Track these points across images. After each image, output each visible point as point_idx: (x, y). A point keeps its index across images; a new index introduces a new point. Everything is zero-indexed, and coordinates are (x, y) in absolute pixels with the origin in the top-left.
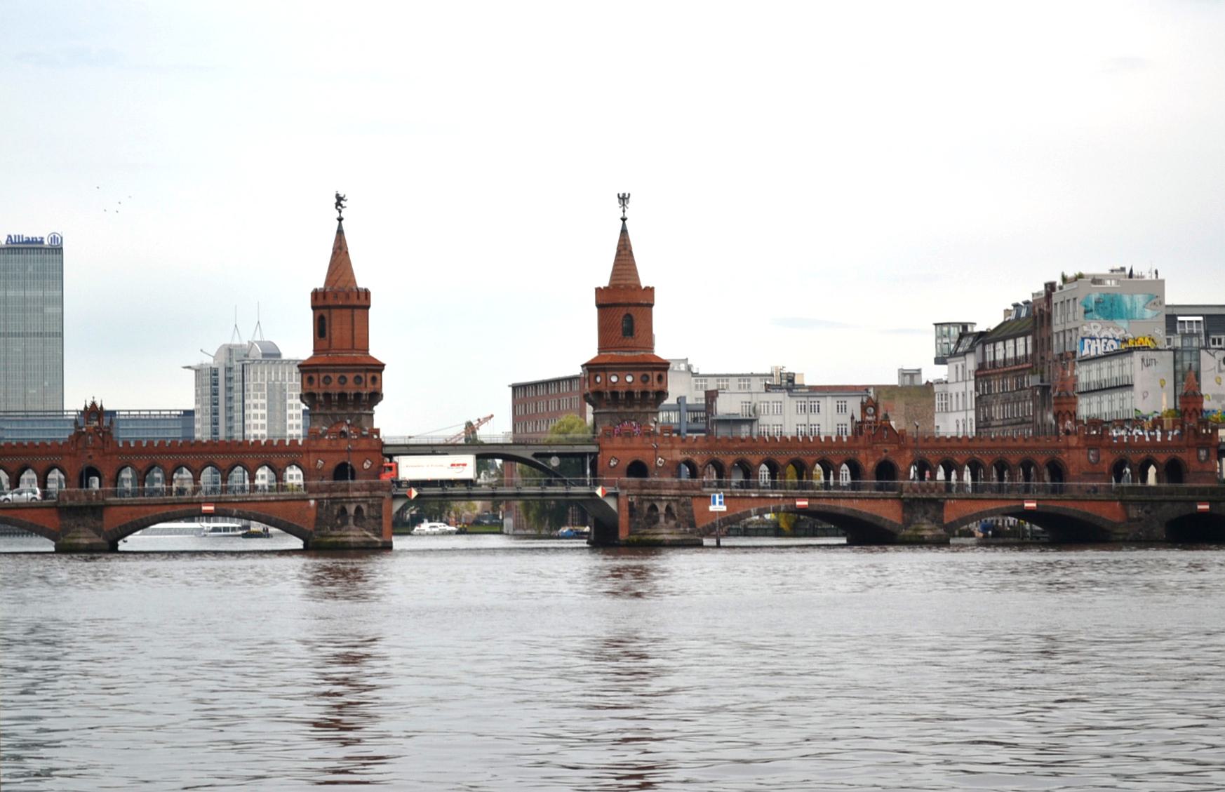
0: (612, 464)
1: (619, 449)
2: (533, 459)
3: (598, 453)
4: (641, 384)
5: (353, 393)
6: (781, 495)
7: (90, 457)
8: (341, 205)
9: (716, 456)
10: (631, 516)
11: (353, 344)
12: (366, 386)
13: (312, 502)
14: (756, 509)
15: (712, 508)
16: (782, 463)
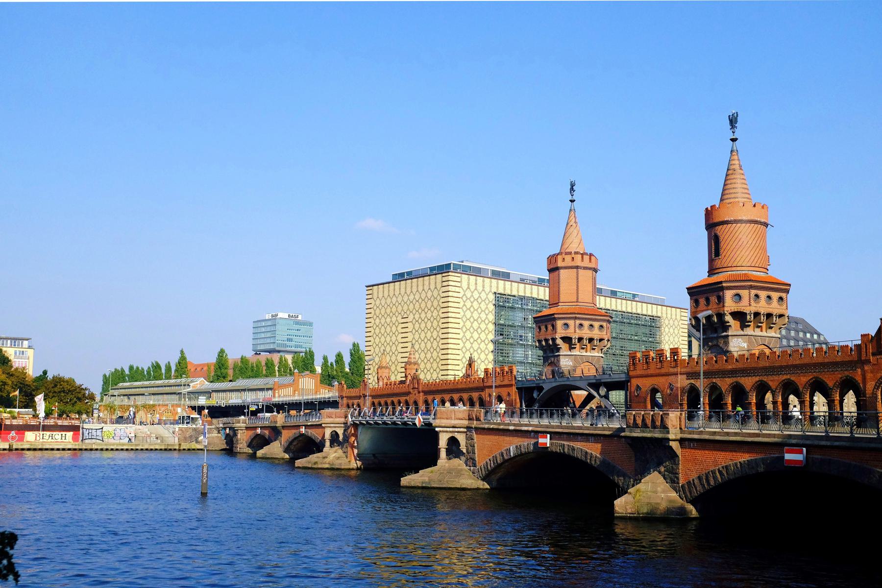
5: (550, 338)
8: (573, 189)
14: (514, 446)
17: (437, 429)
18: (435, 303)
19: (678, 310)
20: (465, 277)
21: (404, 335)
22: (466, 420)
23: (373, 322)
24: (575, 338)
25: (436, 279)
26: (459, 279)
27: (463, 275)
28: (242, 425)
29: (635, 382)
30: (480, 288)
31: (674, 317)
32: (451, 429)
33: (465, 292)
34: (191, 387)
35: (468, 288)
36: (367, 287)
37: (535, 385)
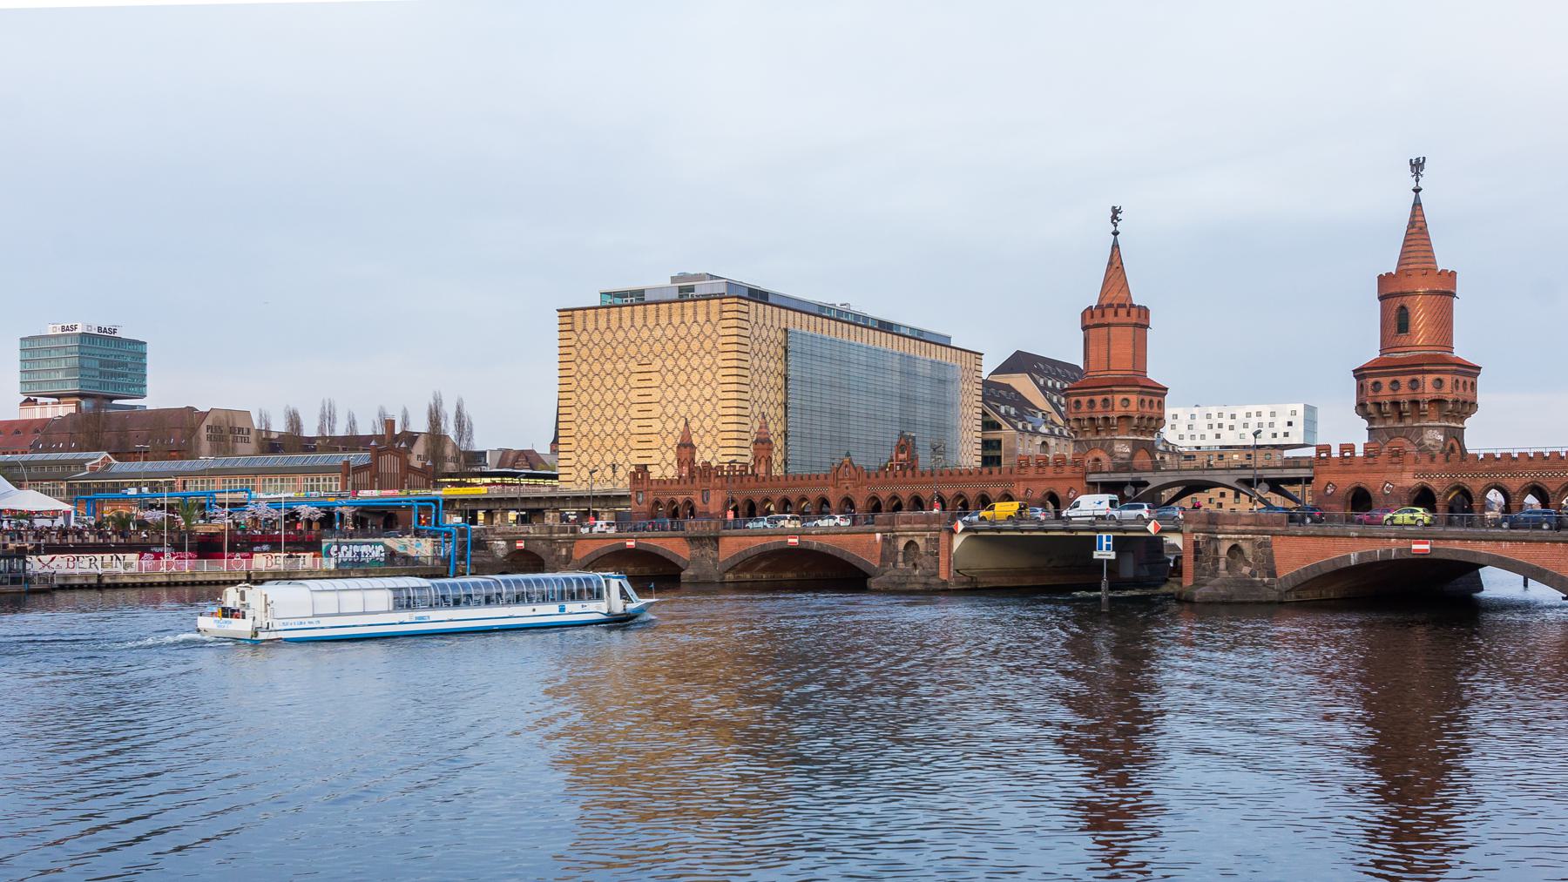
0: (1329, 491)
1: (1337, 472)
2: (1236, 486)
3: (1312, 478)
4: (1409, 392)
5: (1101, 416)
6: (1393, 534)
7: (847, 488)
8: (1117, 218)
9: (1460, 480)
10: (1196, 559)
11: (1109, 366)
12: (1113, 410)
13: (878, 536)
14: (1356, 554)
15: (1096, 555)
16: (1553, 490)
17: (1220, 536)
18: (708, 345)
19: (973, 355)
20: (753, 304)
21: (642, 392)
22: (1204, 523)
23: (575, 368)
24: (1113, 418)
25: (708, 308)
26: (745, 309)
27: (751, 303)
28: (571, 535)
29: (1323, 479)
30: (768, 323)
31: (968, 365)
32: (1236, 536)
33: (752, 328)
34: (88, 468)
35: (756, 323)
36: (558, 311)
37: (1130, 480)
